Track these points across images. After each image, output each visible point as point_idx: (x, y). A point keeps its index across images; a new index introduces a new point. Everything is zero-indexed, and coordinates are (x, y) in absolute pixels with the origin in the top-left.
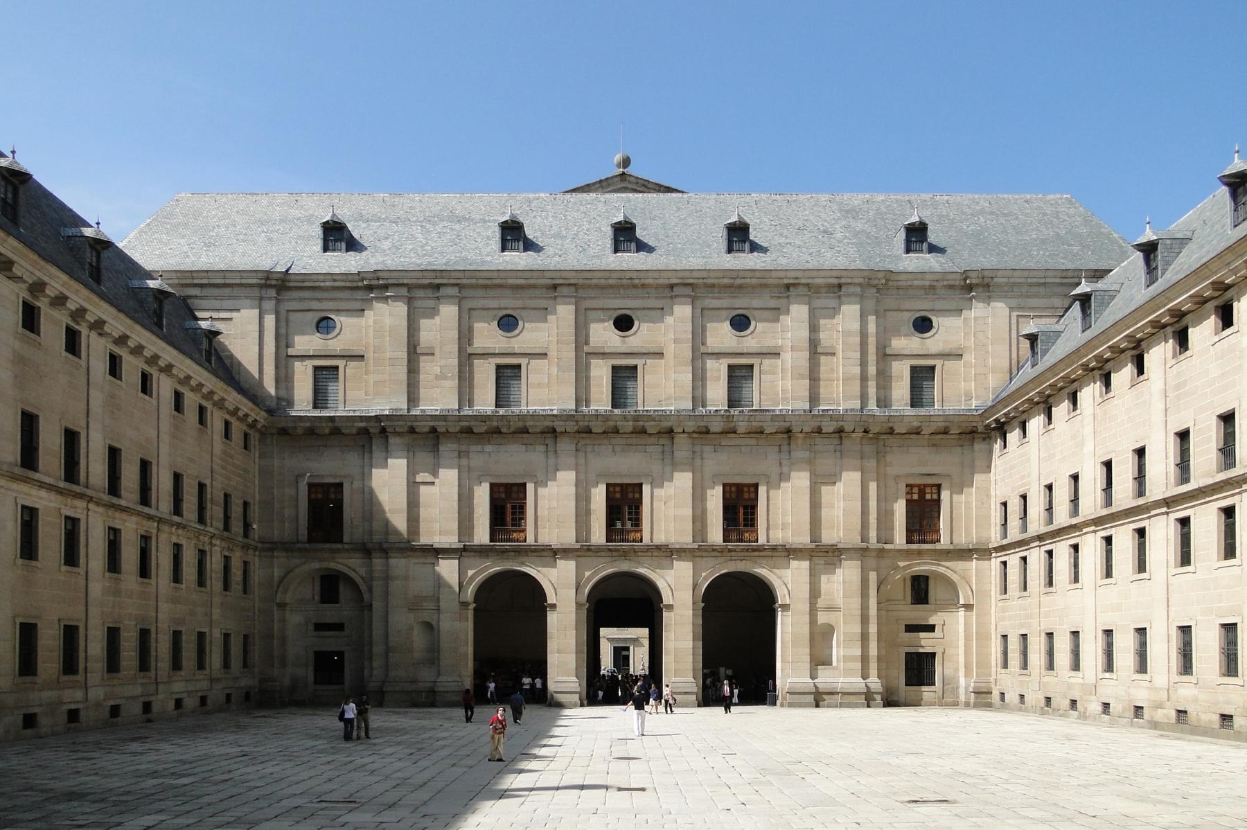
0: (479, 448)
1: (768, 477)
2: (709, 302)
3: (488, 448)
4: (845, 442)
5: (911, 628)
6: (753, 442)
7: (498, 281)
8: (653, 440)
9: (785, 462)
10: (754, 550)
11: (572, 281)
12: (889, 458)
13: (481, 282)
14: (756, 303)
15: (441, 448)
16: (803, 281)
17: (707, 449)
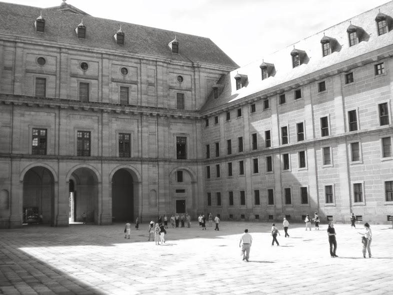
0: (27, 113)
1: (133, 131)
2: (115, 62)
3: (33, 113)
4: (159, 120)
5: (178, 191)
6: (129, 117)
7: (40, 43)
8: (94, 114)
9: (140, 126)
10: (130, 160)
11: (68, 47)
12: (171, 127)
13: (33, 43)
14: (130, 64)
15: (14, 112)
16: (145, 58)
17: (114, 119)
